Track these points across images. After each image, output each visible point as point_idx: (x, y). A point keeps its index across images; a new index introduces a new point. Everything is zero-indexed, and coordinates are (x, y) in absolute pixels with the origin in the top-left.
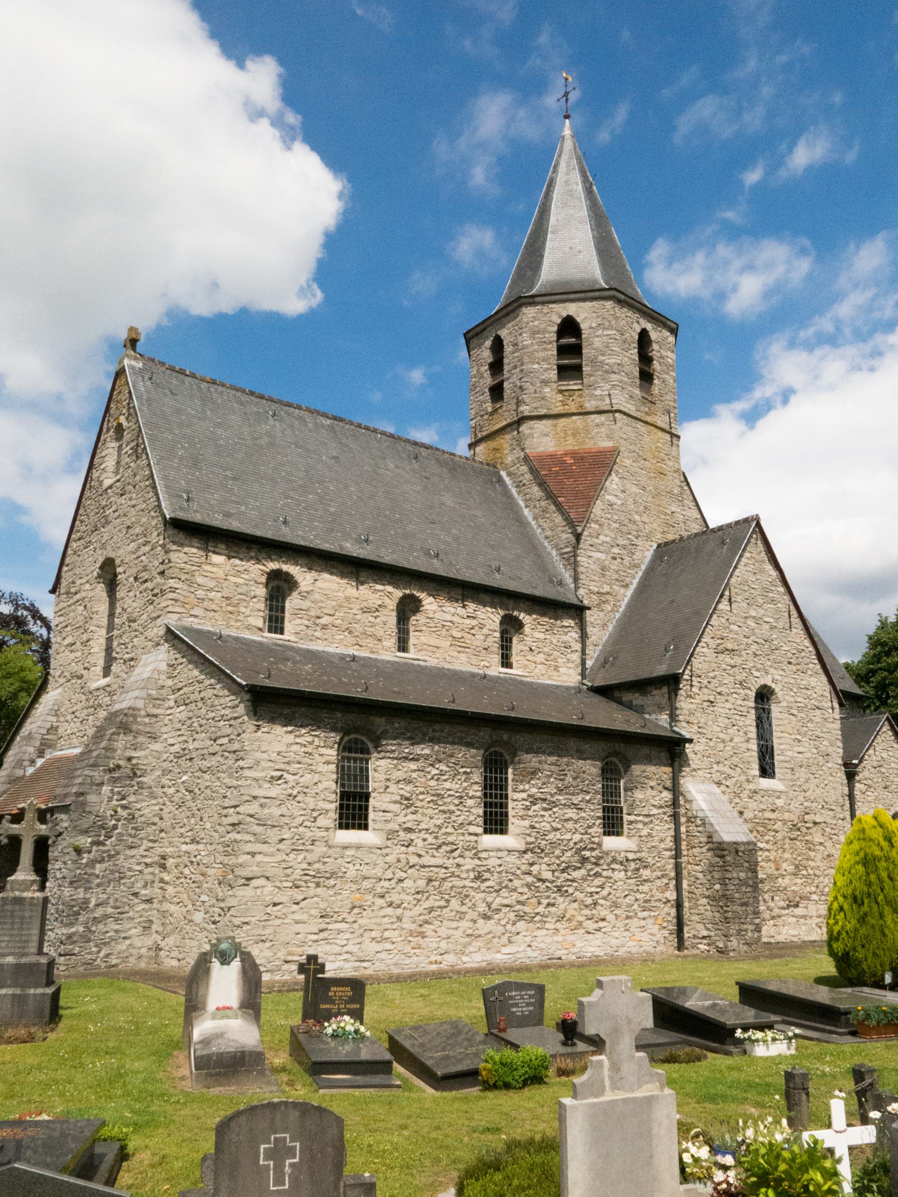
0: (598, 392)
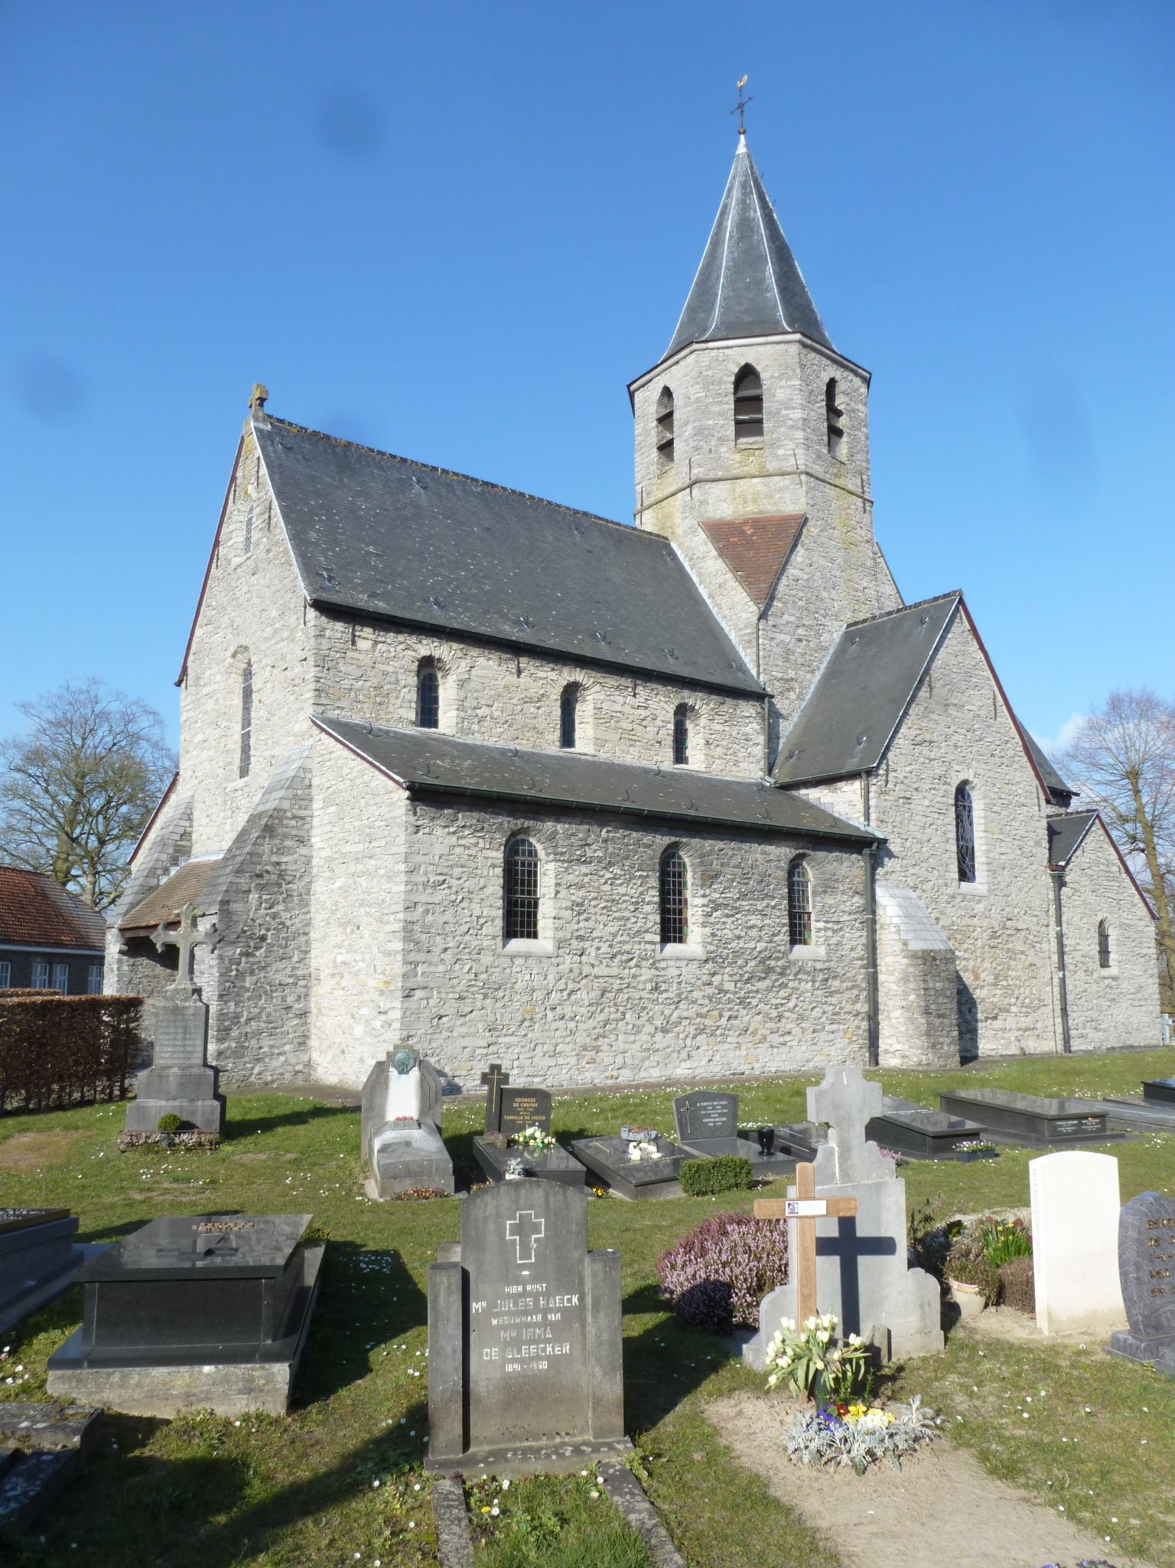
0: (781, 452)
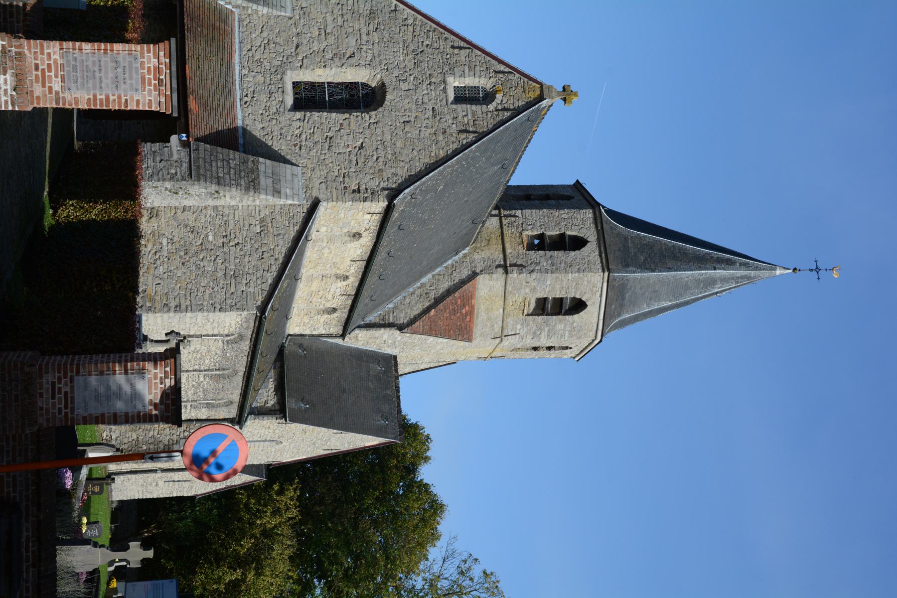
0: (519, 327)
